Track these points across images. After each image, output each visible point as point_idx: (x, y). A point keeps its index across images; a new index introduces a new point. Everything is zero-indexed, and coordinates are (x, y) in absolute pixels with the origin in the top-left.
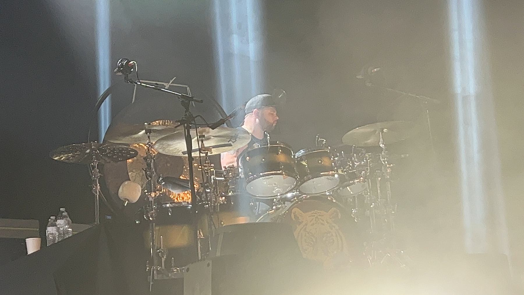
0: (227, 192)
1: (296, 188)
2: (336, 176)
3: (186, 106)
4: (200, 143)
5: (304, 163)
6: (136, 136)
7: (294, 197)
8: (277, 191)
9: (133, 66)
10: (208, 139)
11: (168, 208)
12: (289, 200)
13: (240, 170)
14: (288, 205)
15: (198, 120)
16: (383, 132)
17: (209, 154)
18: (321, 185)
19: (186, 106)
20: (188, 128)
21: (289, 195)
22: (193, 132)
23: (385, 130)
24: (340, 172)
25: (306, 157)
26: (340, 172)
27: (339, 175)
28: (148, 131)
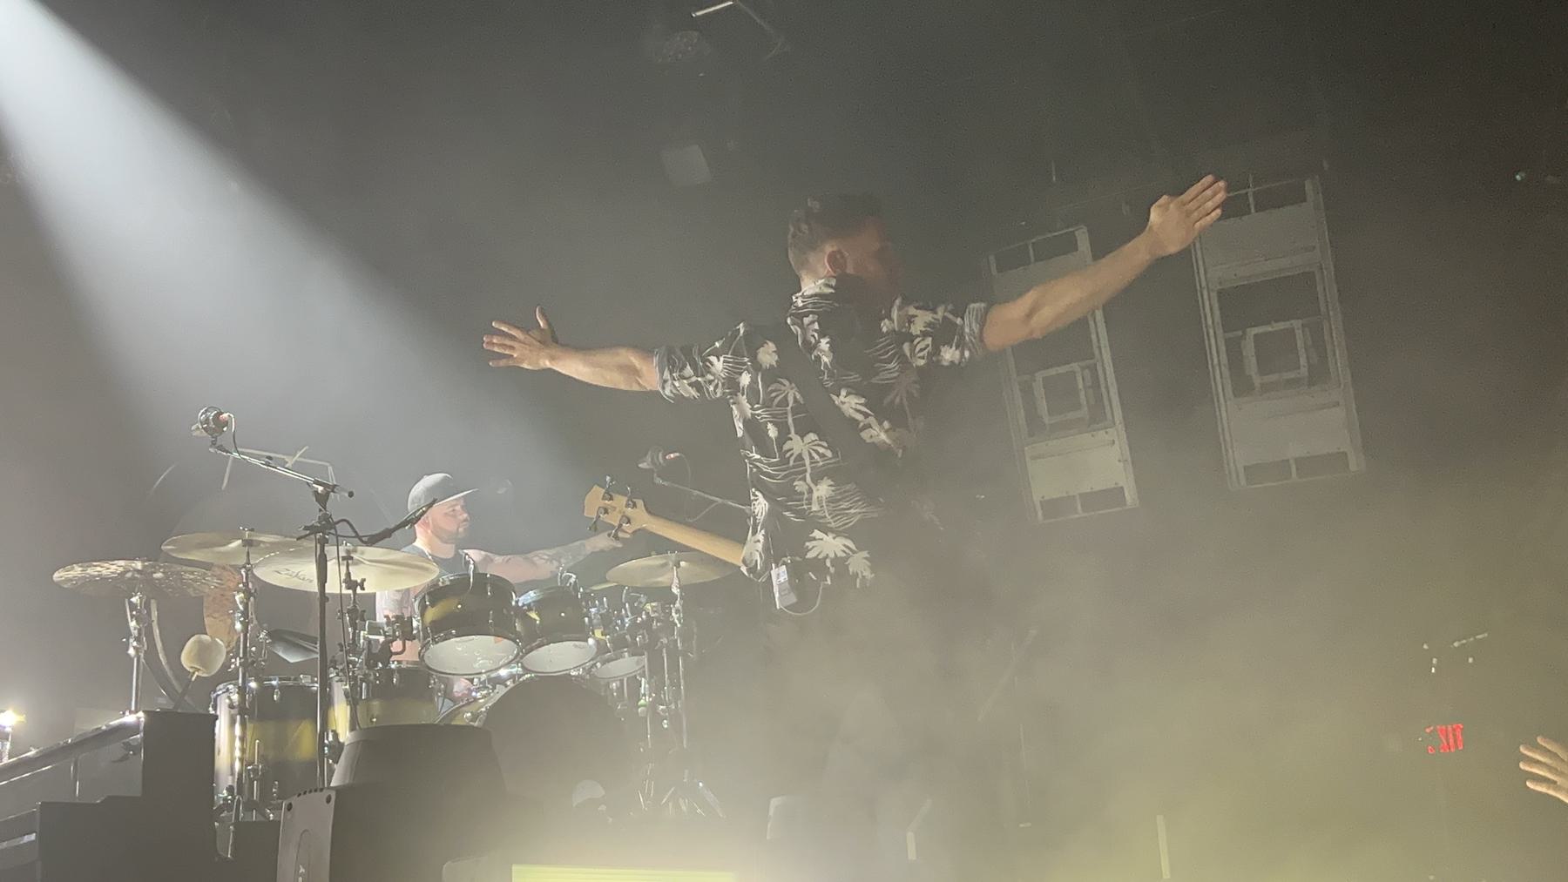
0: (386, 663)
1: (518, 659)
2: (591, 641)
3: (322, 499)
4: (343, 569)
5: (533, 615)
6: (222, 549)
7: (512, 677)
8: (481, 664)
9: (226, 423)
10: (358, 563)
11: (273, 687)
12: (500, 681)
13: (415, 624)
14: (501, 691)
15: (342, 529)
16: (678, 565)
17: (359, 590)
18: (561, 657)
19: (322, 499)
20: (323, 542)
21: (503, 672)
22: (330, 550)
23: (683, 564)
24: (598, 633)
25: (538, 605)
26: (598, 633)
27: (598, 642)
28: (248, 543)
